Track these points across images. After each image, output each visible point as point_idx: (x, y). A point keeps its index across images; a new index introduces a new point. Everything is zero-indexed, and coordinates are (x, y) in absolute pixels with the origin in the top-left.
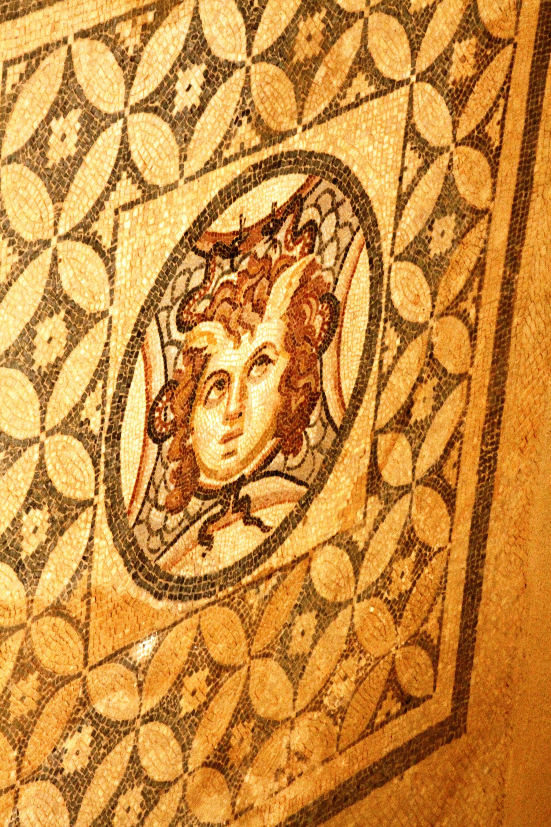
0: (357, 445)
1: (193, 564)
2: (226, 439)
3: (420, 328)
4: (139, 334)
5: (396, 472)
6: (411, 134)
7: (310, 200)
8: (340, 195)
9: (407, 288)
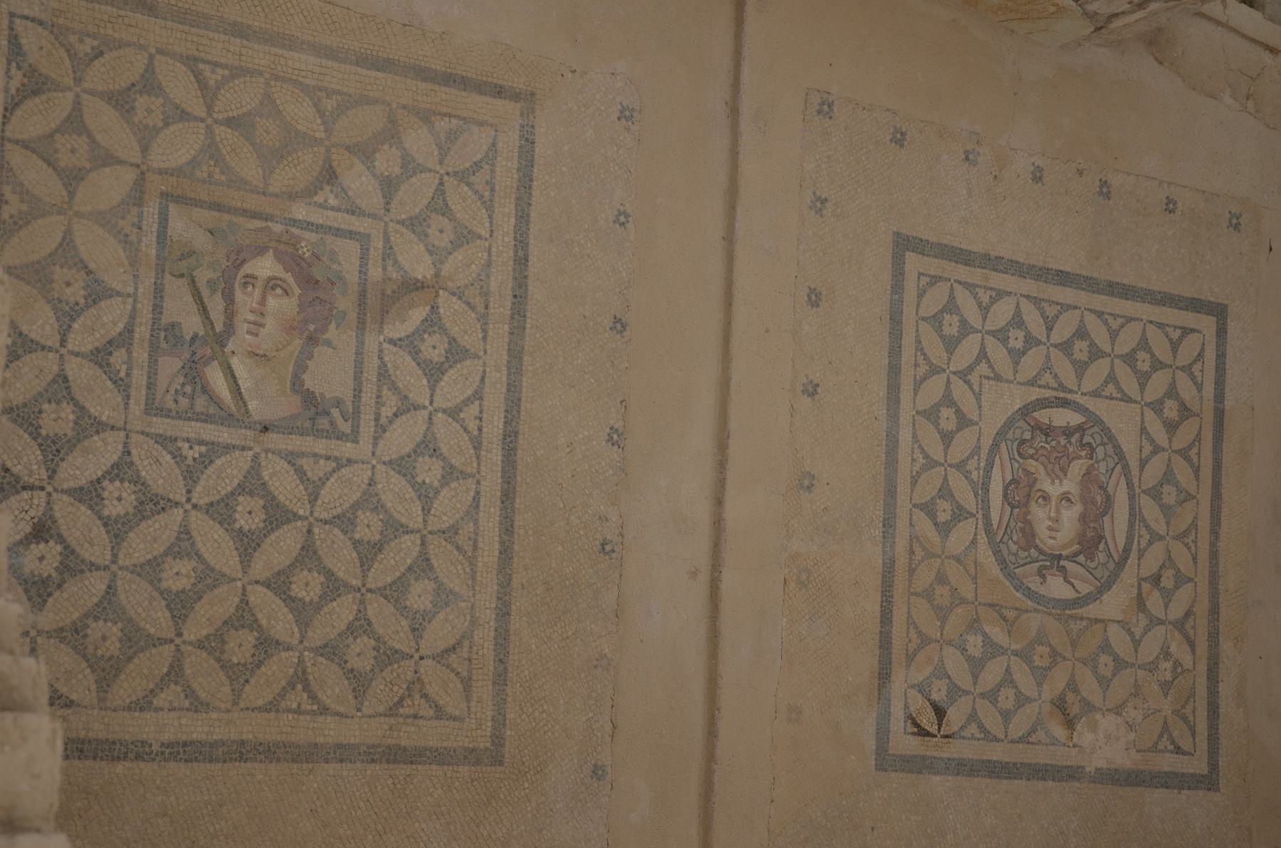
0: (1129, 576)
1: (1034, 583)
2: (1050, 528)
3: (1161, 538)
5: (1154, 602)
6: (1143, 430)
7: (1089, 432)
8: (1106, 440)
9: (1149, 508)
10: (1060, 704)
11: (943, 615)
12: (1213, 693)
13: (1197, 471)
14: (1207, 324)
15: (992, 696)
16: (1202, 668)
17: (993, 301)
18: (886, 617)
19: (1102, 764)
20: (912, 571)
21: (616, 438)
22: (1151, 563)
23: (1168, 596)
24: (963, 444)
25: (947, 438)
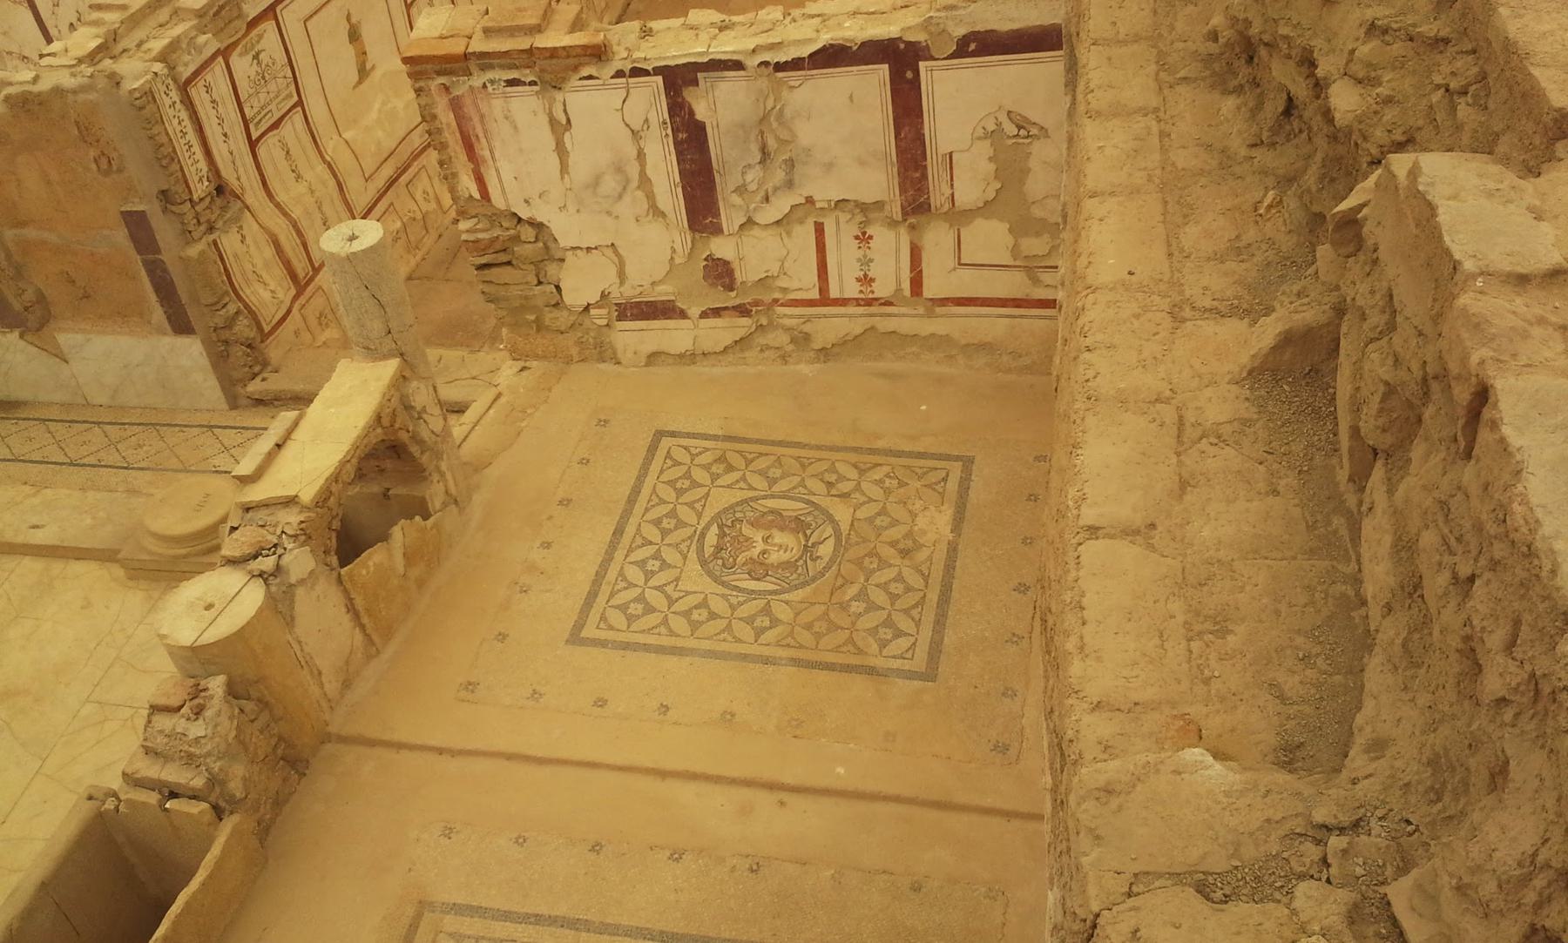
0: (824, 502)
1: (820, 565)
4: (723, 584)
5: (845, 487)
6: (728, 486)
10: (905, 553)
11: (834, 627)
12: (910, 455)
13: (761, 454)
14: (666, 443)
15: (894, 598)
16: (893, 460)
17: (625, 579)
18: (830, 667)
19: (949, 528)
20: (801, 647)
21: (677, 856)
22: (817, 486)
23: (841, 478)
24: (718, 605)
25: (713, 616)
